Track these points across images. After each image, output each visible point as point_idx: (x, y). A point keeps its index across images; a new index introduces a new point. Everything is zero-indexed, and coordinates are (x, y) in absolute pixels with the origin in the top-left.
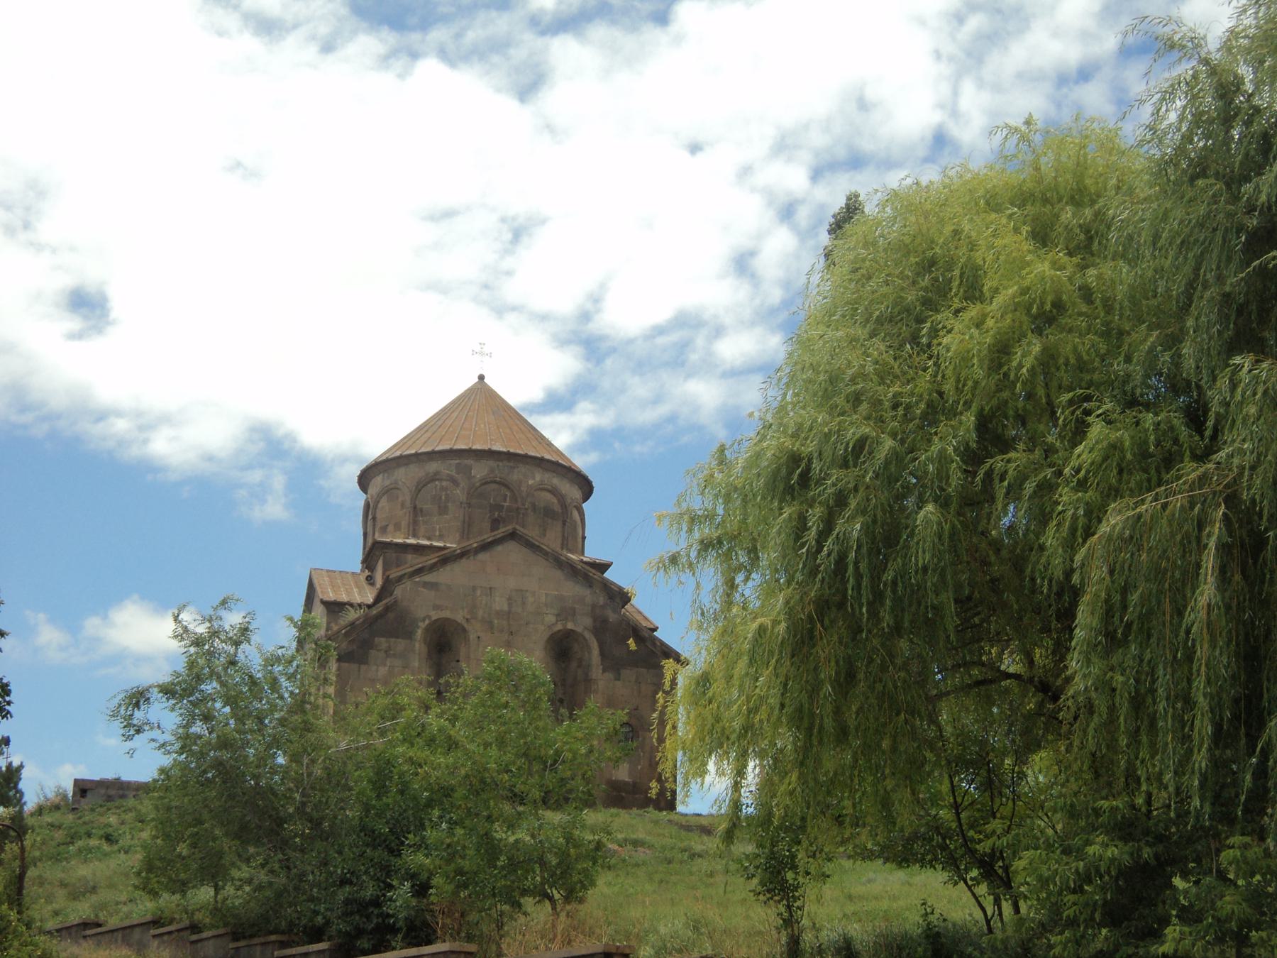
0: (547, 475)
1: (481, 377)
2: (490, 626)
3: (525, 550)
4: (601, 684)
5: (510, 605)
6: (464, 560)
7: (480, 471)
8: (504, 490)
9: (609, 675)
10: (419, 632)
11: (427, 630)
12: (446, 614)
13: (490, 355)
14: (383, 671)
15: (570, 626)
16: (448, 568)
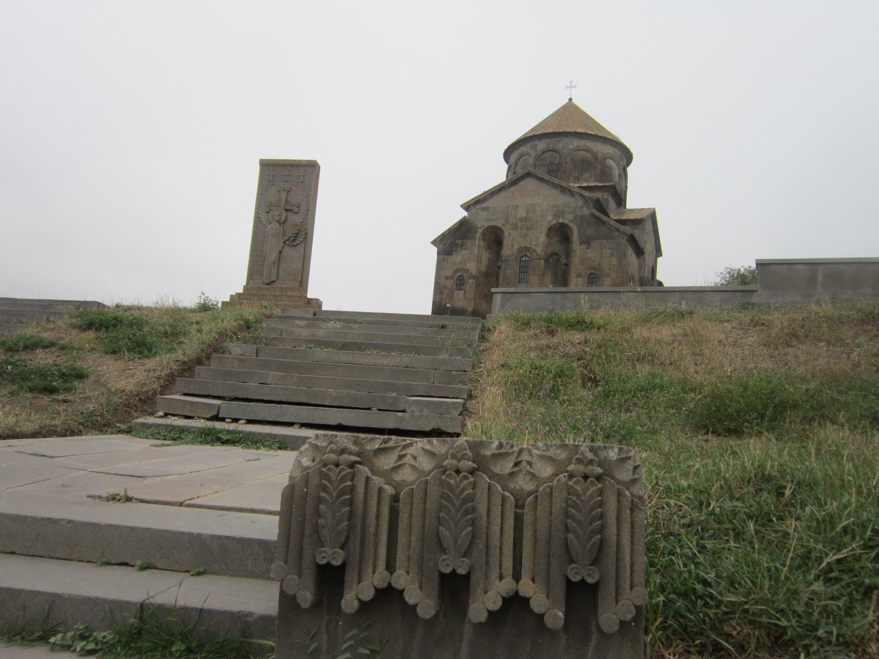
0: (582, 143)
1: (570, 100)
2: (515, 227)
3: (536, 181)
4: (578, 252)
5: (527, 214)
6: (503, 193)
7: (541, 145)
8: (555, 154)
9: (583, 246)
10: (478, 235)
11: (483, 233)
12: (493, 223)
13: (575, 86)
14: (459, 258)
15: (561, 221)
16: (494, 198)
